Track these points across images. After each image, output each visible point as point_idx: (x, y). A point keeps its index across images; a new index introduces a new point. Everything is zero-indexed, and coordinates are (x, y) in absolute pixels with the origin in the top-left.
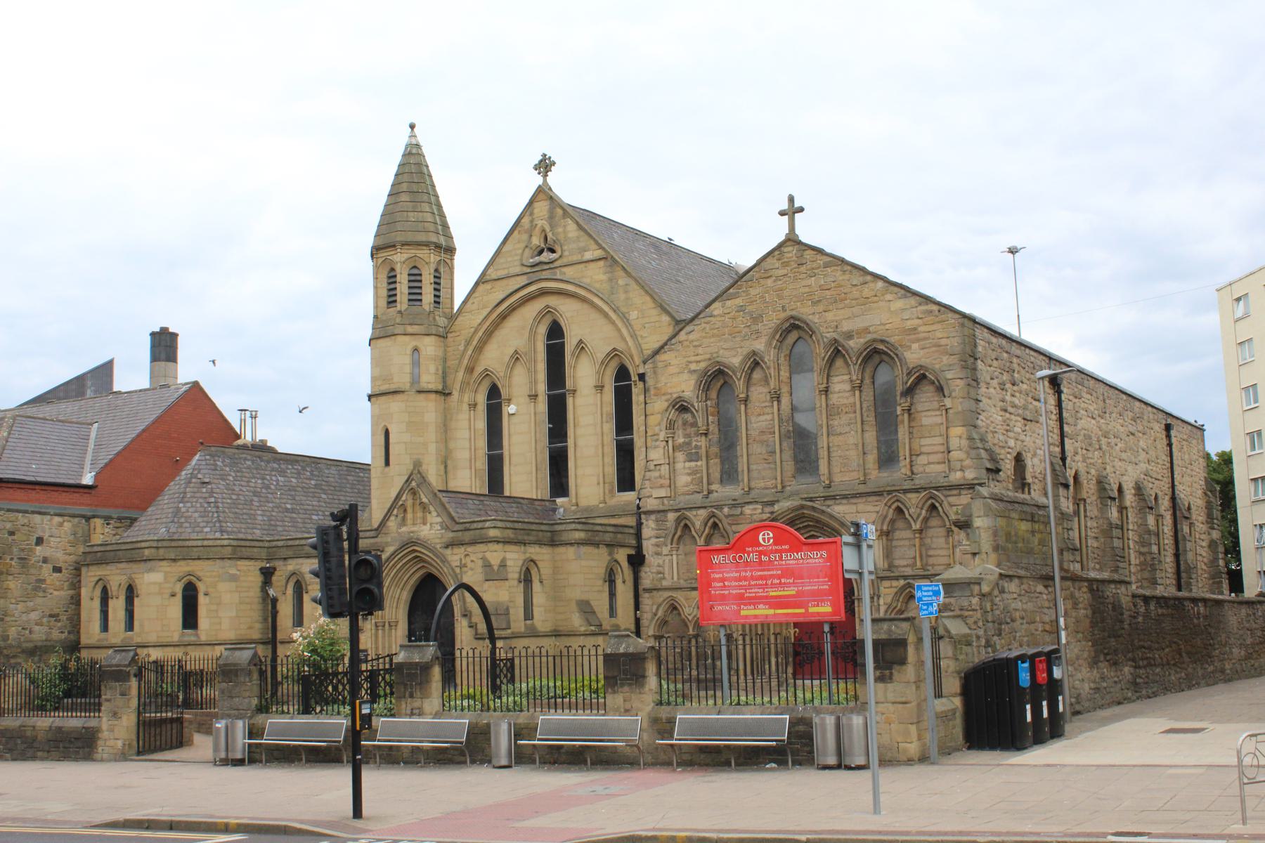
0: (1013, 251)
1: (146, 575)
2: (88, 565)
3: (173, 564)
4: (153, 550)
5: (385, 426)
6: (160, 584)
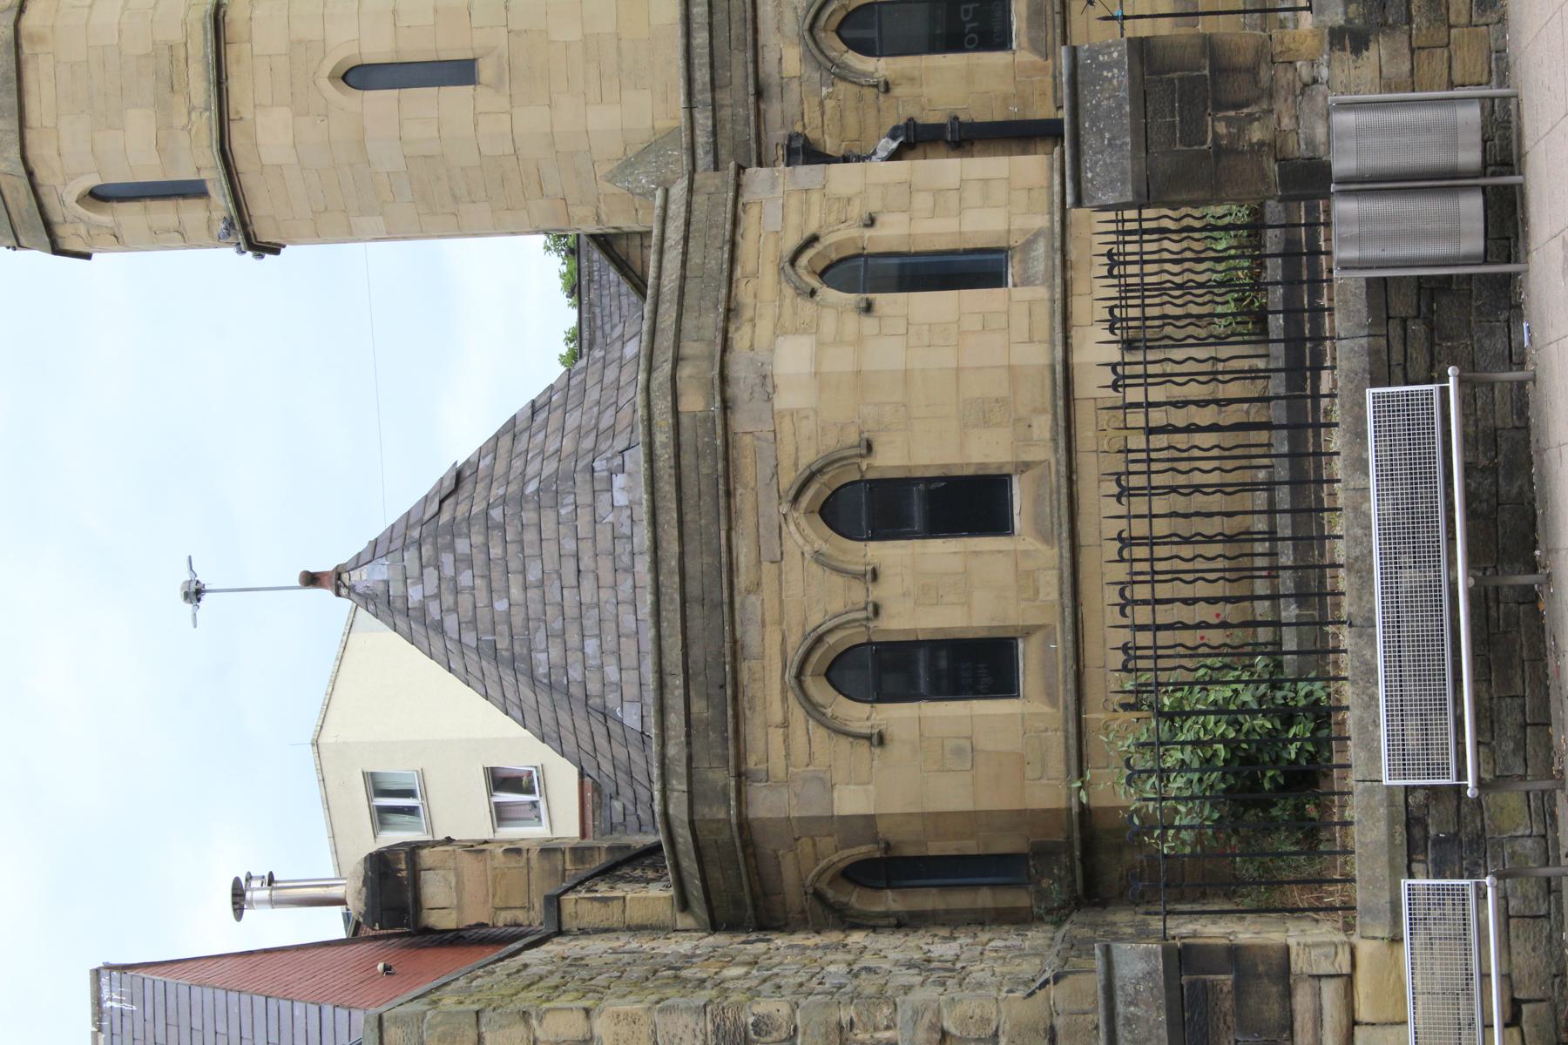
0: (195, 594)
1: (785, 400)
2: (741, 776)
3: (748, 314)
4: (685, 371)
5: (331, 77)
6: (820, 344)
